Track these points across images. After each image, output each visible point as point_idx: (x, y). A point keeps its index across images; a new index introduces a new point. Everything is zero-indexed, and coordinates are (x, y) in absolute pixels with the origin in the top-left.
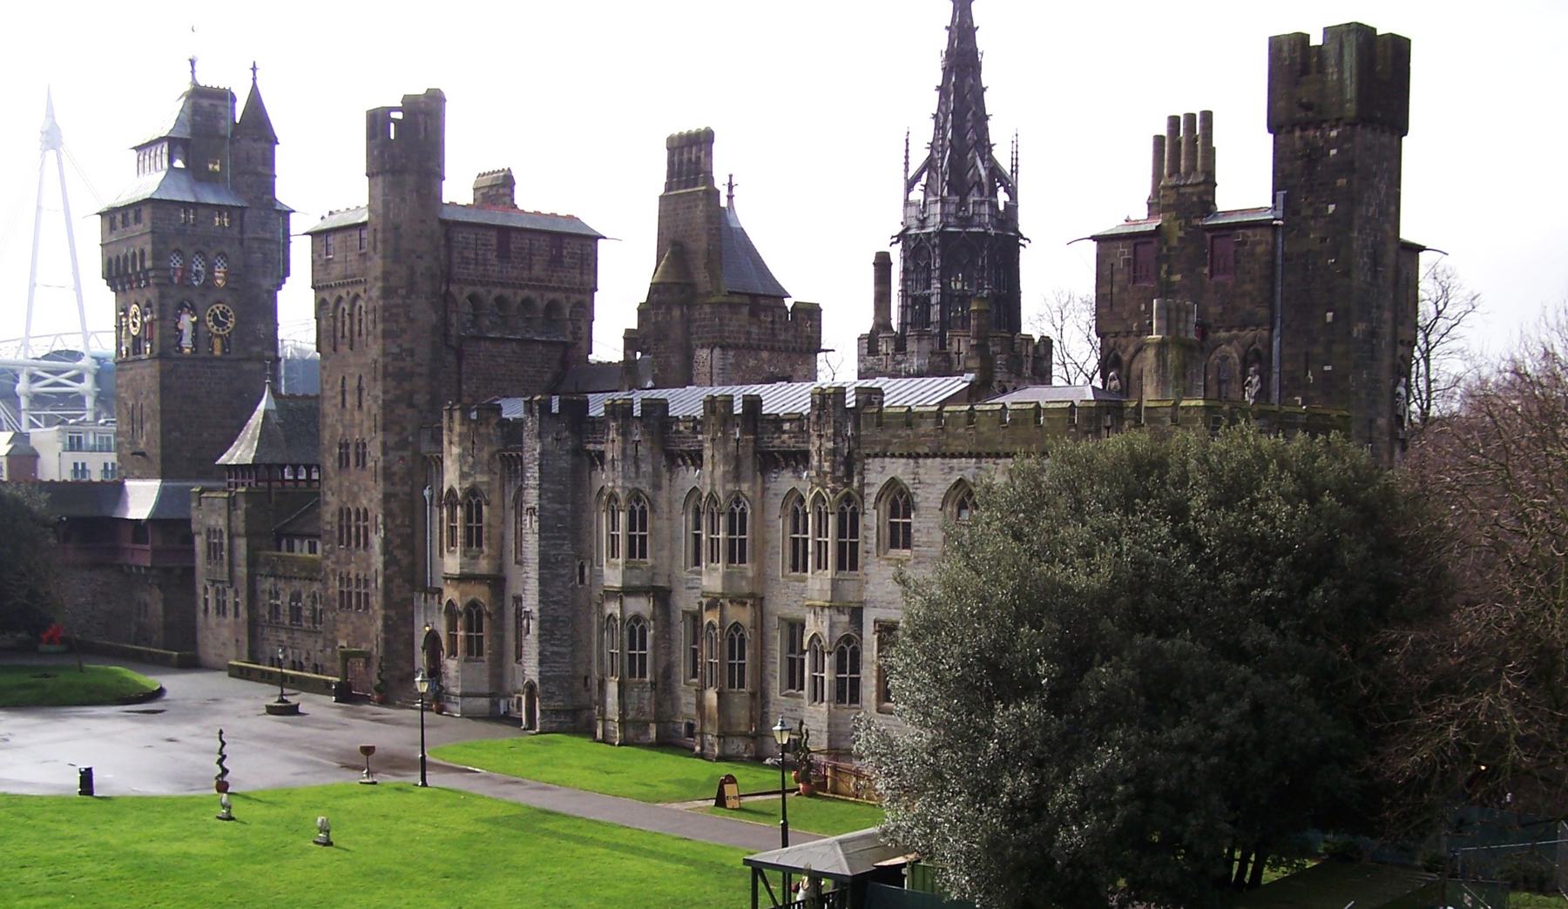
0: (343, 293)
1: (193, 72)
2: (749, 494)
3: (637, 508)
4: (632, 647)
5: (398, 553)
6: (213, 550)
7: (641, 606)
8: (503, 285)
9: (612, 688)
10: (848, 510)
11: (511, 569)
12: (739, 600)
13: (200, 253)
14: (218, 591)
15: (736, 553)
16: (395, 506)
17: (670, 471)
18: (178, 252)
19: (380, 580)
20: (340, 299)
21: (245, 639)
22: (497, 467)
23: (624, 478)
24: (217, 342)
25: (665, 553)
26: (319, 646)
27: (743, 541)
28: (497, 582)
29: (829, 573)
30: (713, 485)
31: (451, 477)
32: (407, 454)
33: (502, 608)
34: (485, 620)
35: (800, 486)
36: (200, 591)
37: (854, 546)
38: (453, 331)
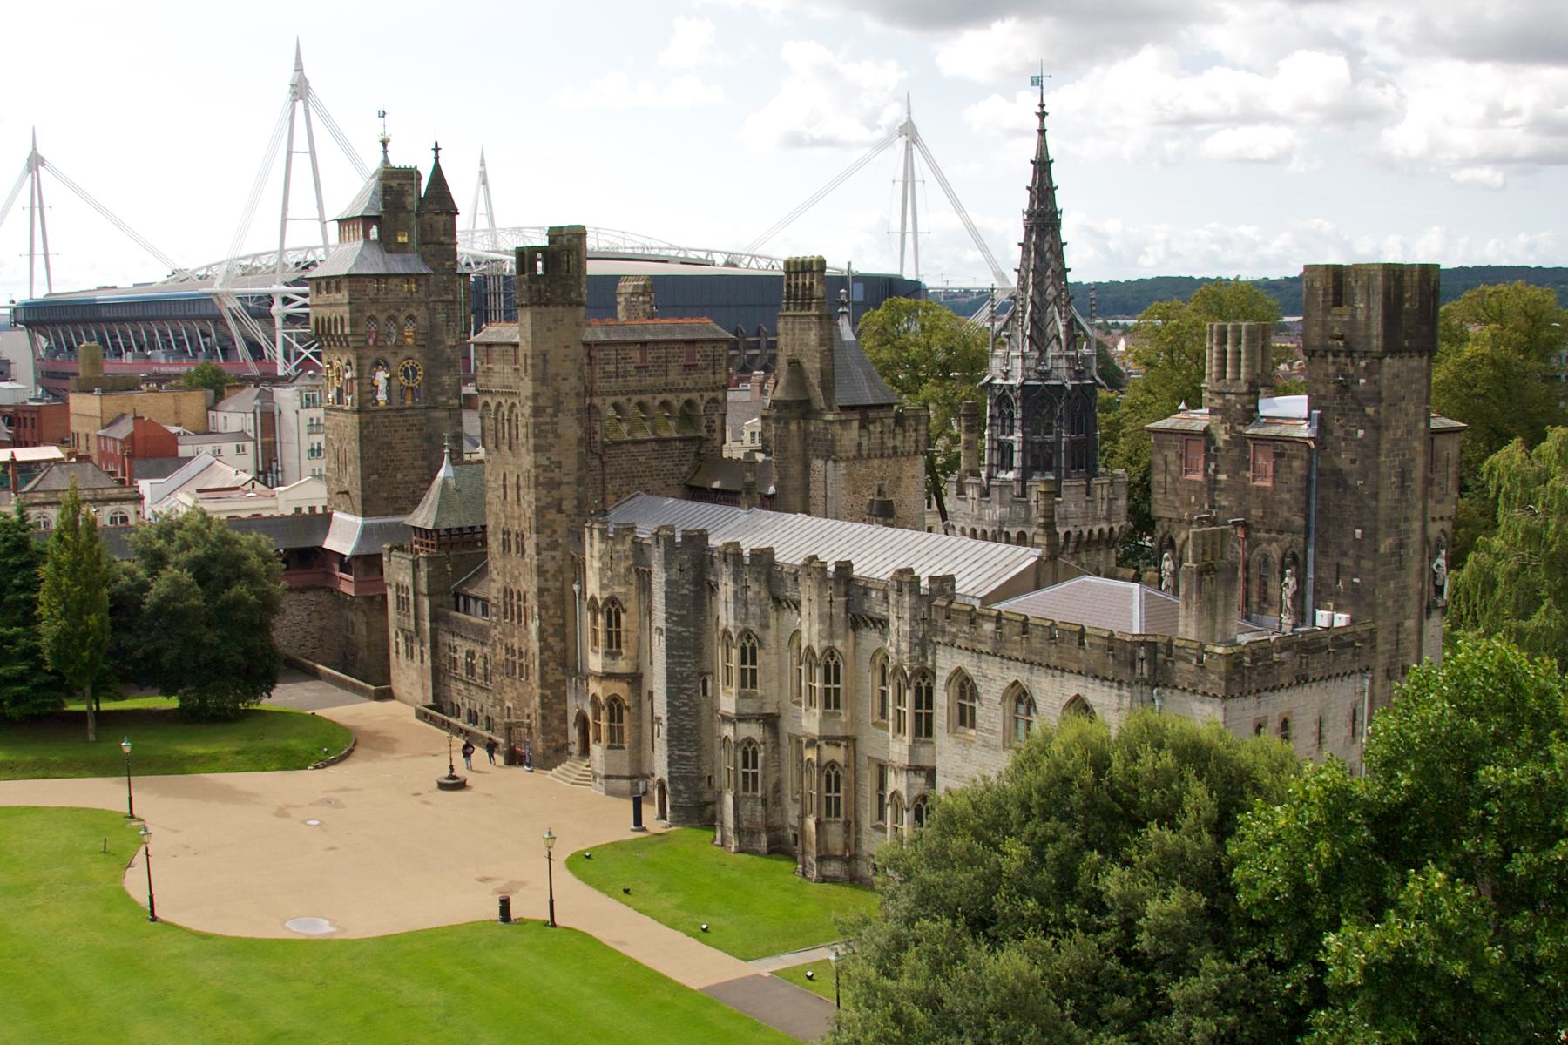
3: (748, 645)
4: (745, 765)
7: (754, 731)
9: (729, 799)
17: (777, 611)
23: (736, 619)
24: (409, 395)
25: (775, 684)
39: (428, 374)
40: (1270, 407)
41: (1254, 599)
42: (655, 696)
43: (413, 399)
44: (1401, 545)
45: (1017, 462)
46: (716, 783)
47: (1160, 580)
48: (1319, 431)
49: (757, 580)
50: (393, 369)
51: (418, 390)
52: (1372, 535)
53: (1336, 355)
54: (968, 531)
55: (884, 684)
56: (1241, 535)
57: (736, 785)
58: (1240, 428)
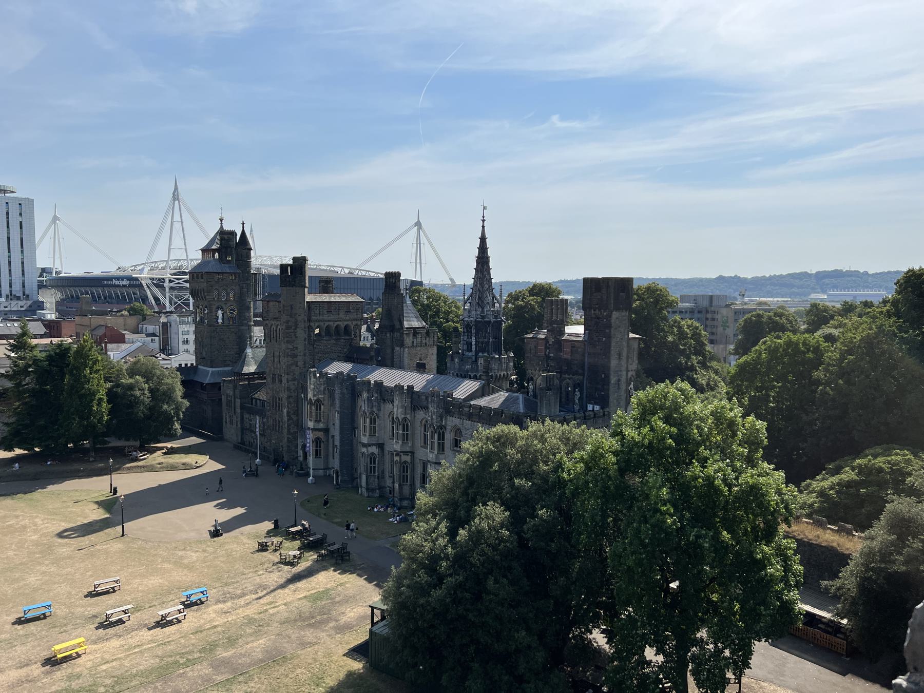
1: (221, 224)
2: (409, 418)
3: (373, 417)
4: (371, 463)
5: (292, 416)
6: (229, 402)
7: (374, 450)
8: (329, 321)
9: (364, 477)
11: (332, 429)
12: (406, 453)
13: (224, 289)
14: (230, 417)
15: (405, 438)
16: (291, 400)
18: (216, 289)
19: (286, 425)
20: (272, 325)
21: (239, 434)
22: (327, 392)
24: (231, 320)
25: (383, 432)
26: (266, 440)
27: (407, 434)
28: (326, 431)
29: (436, 452)
30: (397, 414)
31: (310, 395)
32: (296, 383)
33: (328, 439)
34: (322, 444)
35: (427, 417)
36: (224, 415)
37: (443, 444)
38: (312, 338)
39: (239, 313)
43: (233, 323)
44: (619, 380)
45: (473, 347)
48: (588, 338)
49: (377, 392)
51: (235, 318)
52: (608, 377)
53: (594, 311)
54: (455, 374)
55: (425, 431)
58: (558, 337)
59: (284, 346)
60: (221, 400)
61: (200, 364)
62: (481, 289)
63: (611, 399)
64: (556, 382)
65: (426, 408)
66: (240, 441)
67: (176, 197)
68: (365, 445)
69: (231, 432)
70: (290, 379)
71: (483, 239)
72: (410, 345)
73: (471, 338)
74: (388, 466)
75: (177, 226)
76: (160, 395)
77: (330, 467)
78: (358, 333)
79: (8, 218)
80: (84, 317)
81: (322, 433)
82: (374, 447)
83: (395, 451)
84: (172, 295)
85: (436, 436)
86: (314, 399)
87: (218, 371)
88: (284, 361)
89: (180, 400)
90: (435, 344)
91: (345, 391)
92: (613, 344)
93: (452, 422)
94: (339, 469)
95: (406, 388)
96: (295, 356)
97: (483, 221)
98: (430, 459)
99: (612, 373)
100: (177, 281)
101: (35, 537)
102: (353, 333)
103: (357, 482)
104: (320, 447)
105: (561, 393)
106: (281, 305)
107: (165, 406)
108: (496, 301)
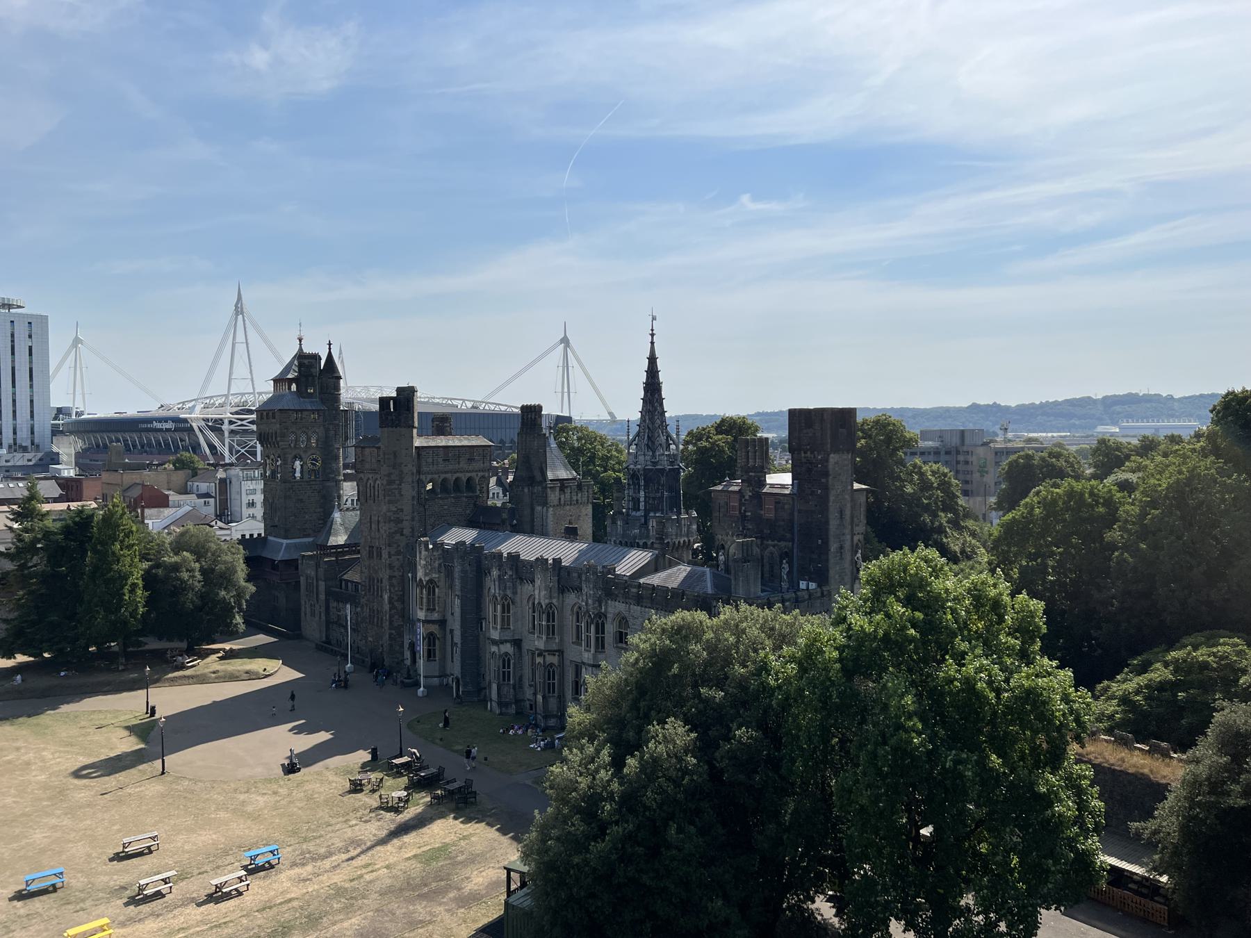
0: (370, 476)
1: (300, 345)
2: (556, 604)
3: (506, 603)
4: (504, 667)
5: (396, 603)
7: (507, 648)
8: (446, 472)
9: (494, 686)
10: (600, 622)
11: (449, 617)
12: (552, 653)
14: (311, 605)
15: (551, 631)
16: (394, 581)
18: (293, 432)
20: (369, 479)
26: (360, 638)
27: (553, 626)
28: (442, 623)
29: (593, 649)
30: (539, 599)
31: (420, 574)
32: (400, 557)
34: (437, 642)
35: (580, 602)
36: (303, 603)
37: (603, 638)
38: (422, 496)
40: (772, 479)
41: (766, 575)
42: (455, 632)
43: (315, 476)
44: (841, 547)
45: (642, 504)
46: (487, 679)
47: (718, 566)
48: (798, 491)
49: (511, 569)
50: (305, 460)
52: (826, 543)
53: (805, 453)
55: (578, 622)
56: (759, 542)
57: (499, 678)
59: (384, 508)
60: (298, 583)
61: (270, 534)
62: (650, 426)
63: (832, 573)
64: (756, 551)
65: (579, 589)
66: (324, 639)
67: (239, 310)
68: (495, 642)
69: (312, 627)
70: (392, 553)
71: (652, 360)
72: (556, 502)
73: (639, 492)
74: (527, 672)
75: (241, 348)
76: (215, 577)
77: (448, 673)
78: (485, 488)
79: (13, 341)
80: (113, 473)
81: (437, 626)
82: (508, 645)
83: (537, 649)
84: (233, 441)
85: (593, 628)
86: (425, 579)
87: (295, 543)
88: (385, 528)
89: (243, 583)
90: (590, 501)
91: (468, 568)
92: (832, 498)
93: (615, 607)
94: (460, 676)
95: (551, 562)
96: (399, 521)
97: (652, 335)
98: (585, 661)
99: (832, 539)
100: (240, 423)
101: (42, 778)
102: (478, 487)
103: (485, 695)
104: (434, 645)
105: (763, 566)
106: (381, 453)
107: (223, 593)
108: (671, 442)
